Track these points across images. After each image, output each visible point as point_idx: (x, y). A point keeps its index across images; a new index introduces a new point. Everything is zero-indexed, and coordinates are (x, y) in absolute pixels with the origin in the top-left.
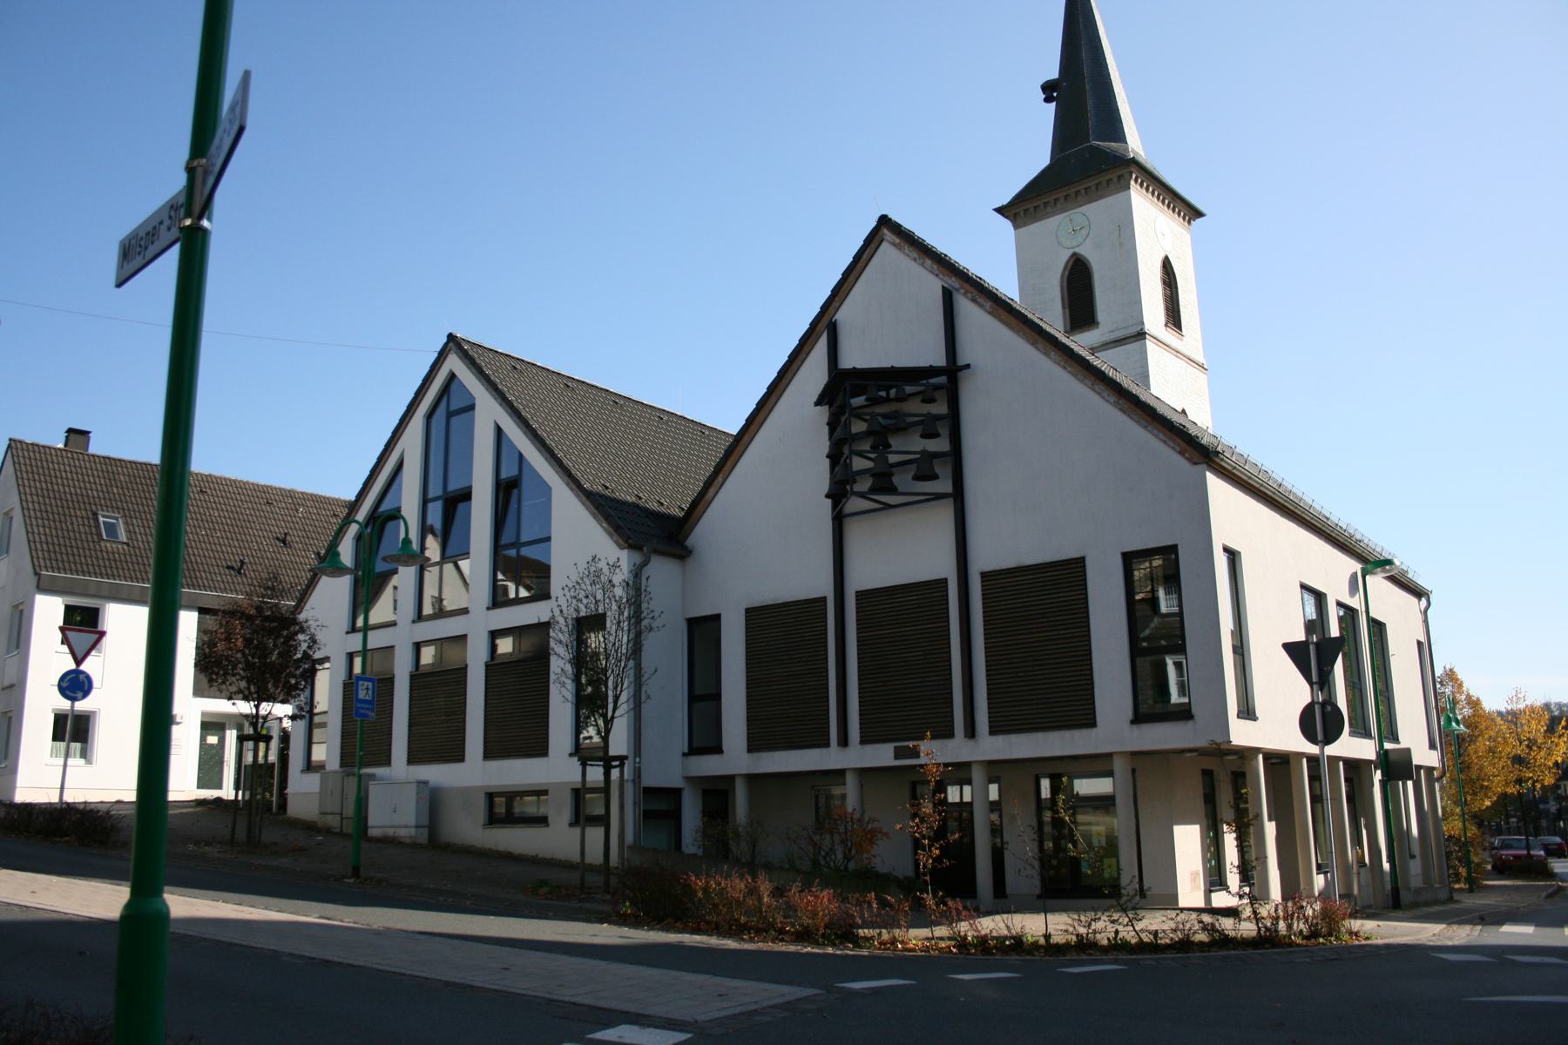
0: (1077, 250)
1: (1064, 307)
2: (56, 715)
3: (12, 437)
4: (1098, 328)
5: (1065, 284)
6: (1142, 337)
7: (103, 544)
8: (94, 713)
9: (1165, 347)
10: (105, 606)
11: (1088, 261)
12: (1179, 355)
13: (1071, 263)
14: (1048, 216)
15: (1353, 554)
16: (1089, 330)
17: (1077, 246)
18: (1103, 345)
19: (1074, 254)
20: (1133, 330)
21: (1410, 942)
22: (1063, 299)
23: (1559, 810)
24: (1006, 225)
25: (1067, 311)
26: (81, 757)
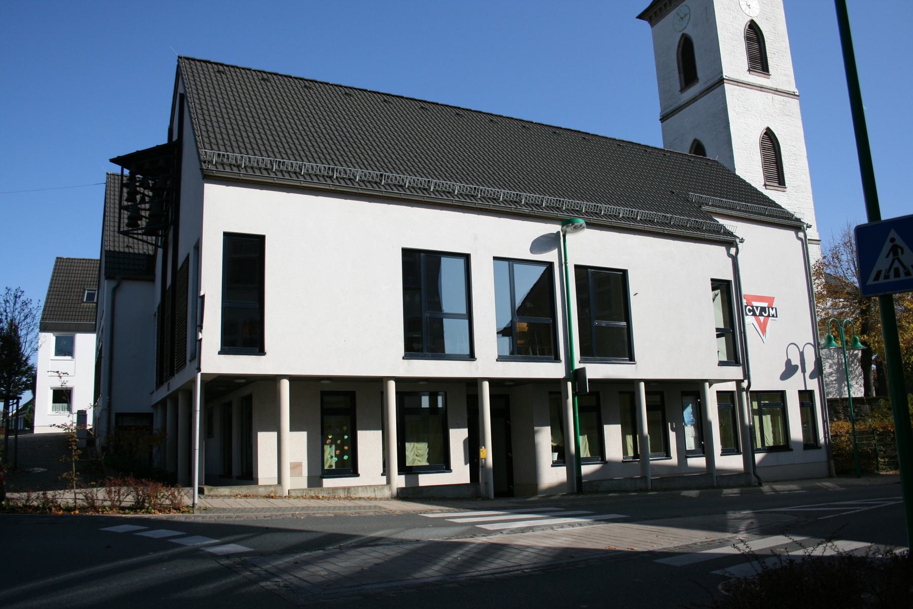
0: (684, 32)
1: (679, 73)
2: (54, 390)
3: (58, 256)
4: (698, 82)
5: (680, 57)
6: (722, 82)
7: (82, 304)
8: (72, 388)
9: (747, 86)
10: (74, 335)
11: (689, 36)
12: (763, 89)
13: (682, 41)
14: (668, 12)
15: (524, 216)
16: (694, 85)
17: (684, 29)
18: (701, 94)
19: (683, 35)
20: (717, 79)
21: (378, 536)
22: (679, 67)
23: (110, 501)
24: (645, 24)
25: (682, 75)
26: (68, 411)
